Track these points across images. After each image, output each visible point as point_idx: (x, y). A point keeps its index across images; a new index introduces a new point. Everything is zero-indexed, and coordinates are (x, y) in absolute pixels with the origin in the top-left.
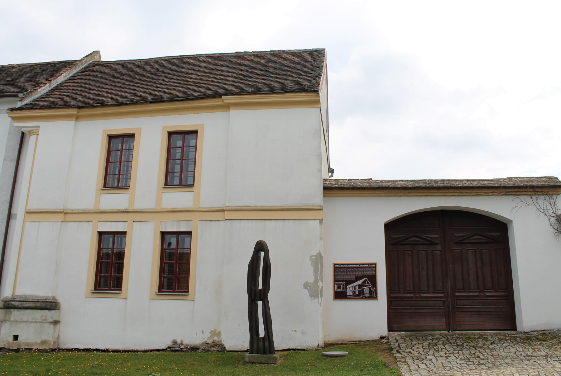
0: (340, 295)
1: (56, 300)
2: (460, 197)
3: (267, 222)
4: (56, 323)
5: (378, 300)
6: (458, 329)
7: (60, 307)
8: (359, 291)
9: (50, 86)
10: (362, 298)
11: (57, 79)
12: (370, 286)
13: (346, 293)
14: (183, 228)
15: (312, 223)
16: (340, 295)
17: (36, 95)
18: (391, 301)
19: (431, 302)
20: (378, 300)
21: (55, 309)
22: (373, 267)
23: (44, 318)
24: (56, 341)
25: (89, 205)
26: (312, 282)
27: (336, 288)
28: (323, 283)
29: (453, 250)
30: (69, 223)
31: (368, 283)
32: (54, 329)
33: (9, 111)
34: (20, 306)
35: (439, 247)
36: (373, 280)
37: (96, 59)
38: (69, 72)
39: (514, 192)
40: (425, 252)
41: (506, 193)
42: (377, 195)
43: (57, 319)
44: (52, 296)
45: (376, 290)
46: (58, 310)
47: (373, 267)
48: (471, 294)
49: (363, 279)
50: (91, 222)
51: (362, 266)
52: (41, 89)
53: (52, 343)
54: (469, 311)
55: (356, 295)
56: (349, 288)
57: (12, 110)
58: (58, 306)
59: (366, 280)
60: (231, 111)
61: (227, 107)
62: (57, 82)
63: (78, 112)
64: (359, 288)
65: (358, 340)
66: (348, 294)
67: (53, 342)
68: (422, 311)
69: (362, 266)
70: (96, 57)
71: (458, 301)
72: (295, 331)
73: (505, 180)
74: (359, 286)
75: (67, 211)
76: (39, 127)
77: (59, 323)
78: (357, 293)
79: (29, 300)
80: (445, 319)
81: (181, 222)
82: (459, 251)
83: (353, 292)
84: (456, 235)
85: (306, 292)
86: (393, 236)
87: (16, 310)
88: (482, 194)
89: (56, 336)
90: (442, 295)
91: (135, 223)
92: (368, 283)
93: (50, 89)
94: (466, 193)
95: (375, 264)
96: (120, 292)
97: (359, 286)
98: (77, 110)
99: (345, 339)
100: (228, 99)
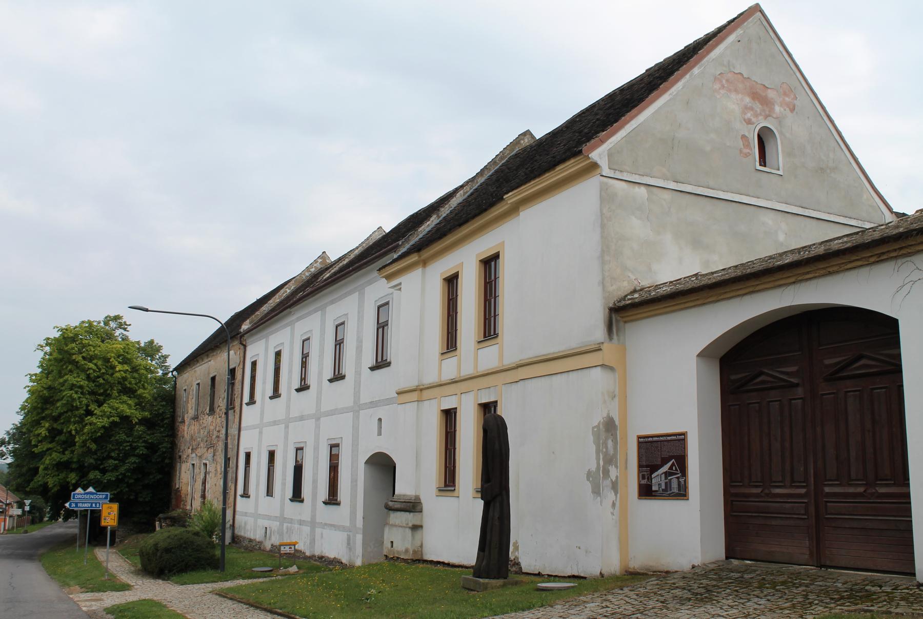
0: (646, 492)
1: (420, 499)
2: (797, 286)
3: (554, 377)
4: (416, 528)
5: (688, 499)
6: (828, 563)
7: (422, 509)
8: (666, 483)
9: (439, 217)
10: (669, 495)
11: (450, 203)
12: (678, 473)
13: (650, 486)
14: (492, 399)
15: (594, 370)
16: (646, 492)
17: (417, 237)
18: (732, 501)
19: (788, 505)
20: (688, 499)
21: (413, 511)
22: (680, 439)
23: (407, 522)
24: (418, 551)
25: (431, 378)
26: (594, 470)
27: (641, 479)
28: (618, 470)
29: (823, 395)
30: (425, 402)
31: (676, 470)
32: (413, 536)
33: (378, 272)
34: (393, 508)
35: (800, 391)
36: (681, 462)
37: (526, 142)
38: (470, 186)
39: (895, 250)
40: (778, 403)
41: (879, 257)
42: (682, 306)
43: (418, 523)
44: (414, 494)
45: (685, 481)
46: (421, 512)
47: (680, 439)
48: (851, 490)
49: (669, 462)
50: (434, 400)
51: (669, 438)
52: (423, 227)
53: (411, 552)
54: (847, 526)
55: (663, 490)
56: (656, 477)
57: (379, 270)
58: (418, 508)
59: (673, 464)
60: (521, 213)
61: (515, 209)
62: (451, 207)
63: (420, 257)
64: (666, 478)
65: (666, 570)
66: (654, 489)
67: (413, 551)
68: (774, 523)
69: (669, 438)
70: (522, 142)
71: (828, 504)
72: (579, 548)
73: (889, 225)
74: (667, 474)
75: (422, 387)
76: (400, 284)
77: (421, 528)
78: (663, 487)
79: (399, 500)
80: (809, 541)
81: (492, 389)
82: (833, 396)
83: (659, 484)
84: (827, 362)
85: (588, 486)
86: (733, 377)
87: (392, 512)
88: (835, 268)
89: (419, 544)
90: (803, 491)
91: (462, 395)
92: (676, 470)
93: (438, 221)
94: (808, 273)
95: (684, 434)
96: (453, 489)
97: (665, 473)
98: (416, 255)
99: (651, 566)
100: (511, 198)
